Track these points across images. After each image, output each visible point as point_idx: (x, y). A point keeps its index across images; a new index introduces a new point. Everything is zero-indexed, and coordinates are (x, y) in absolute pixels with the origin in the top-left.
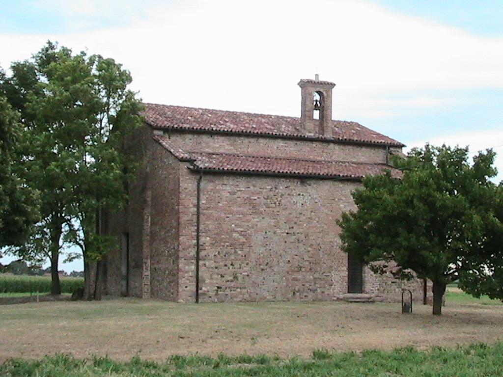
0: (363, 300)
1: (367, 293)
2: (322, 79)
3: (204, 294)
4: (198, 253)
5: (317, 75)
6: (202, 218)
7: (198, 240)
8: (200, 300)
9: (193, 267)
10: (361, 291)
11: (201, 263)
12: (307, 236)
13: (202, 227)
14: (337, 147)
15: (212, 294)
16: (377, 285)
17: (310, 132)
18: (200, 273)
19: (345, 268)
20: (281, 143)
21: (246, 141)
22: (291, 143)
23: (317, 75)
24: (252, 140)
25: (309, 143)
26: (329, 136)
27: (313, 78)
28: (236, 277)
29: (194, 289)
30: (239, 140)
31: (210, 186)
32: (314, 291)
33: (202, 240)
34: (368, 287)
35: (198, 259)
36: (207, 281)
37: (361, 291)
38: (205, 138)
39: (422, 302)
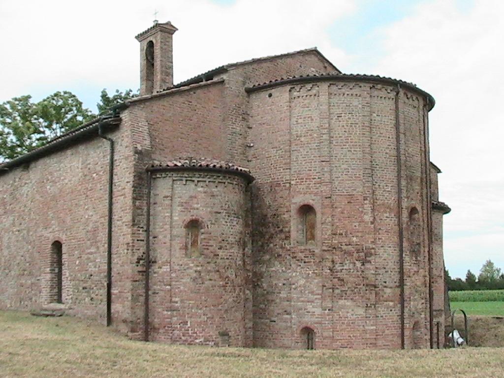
0: (47, 313)
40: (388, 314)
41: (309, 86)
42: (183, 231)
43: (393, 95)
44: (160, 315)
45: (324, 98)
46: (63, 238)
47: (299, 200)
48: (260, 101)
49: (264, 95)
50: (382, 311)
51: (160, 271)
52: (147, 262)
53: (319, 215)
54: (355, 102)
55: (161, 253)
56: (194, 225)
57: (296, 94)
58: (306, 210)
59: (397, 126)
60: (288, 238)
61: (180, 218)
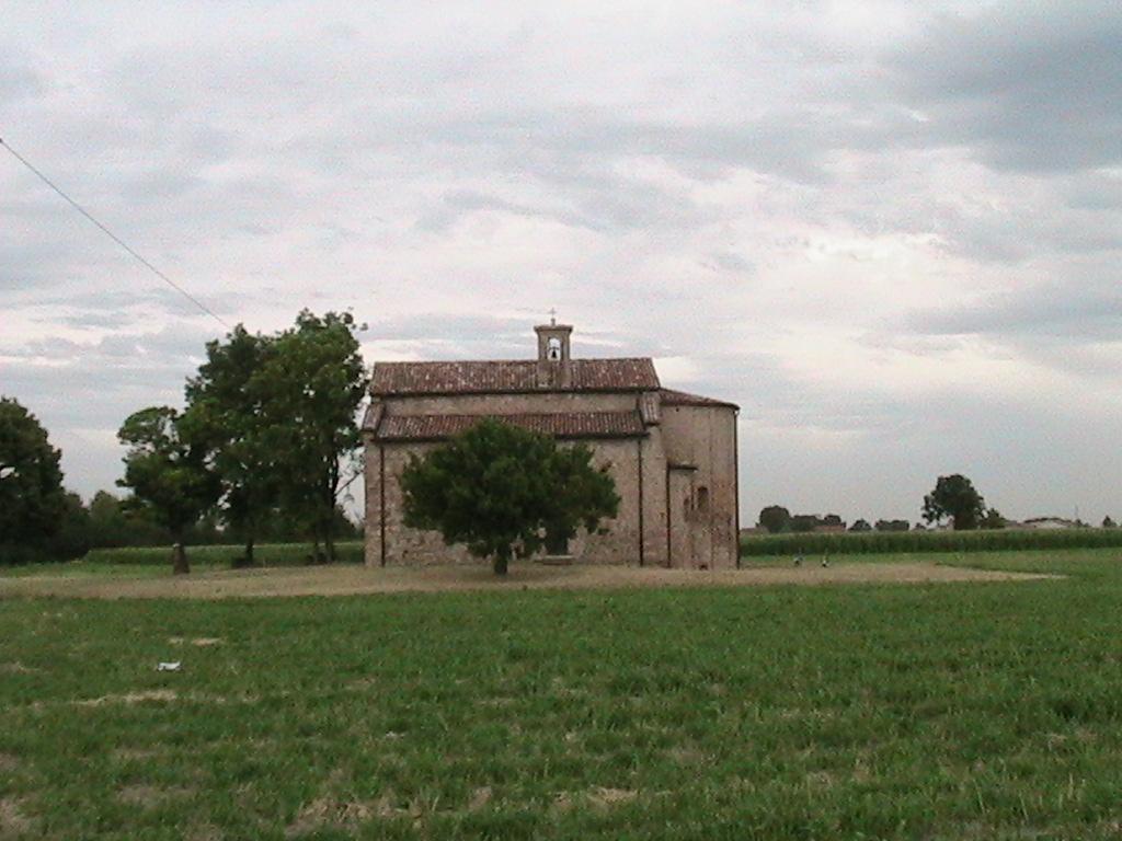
1: (571, 554)
2: (559, 322)
3: (391, 558)
4: (383, 519)
5: (553, 320)
6: (386, 485)
7: (383, 505)
8: (387, 564)
9: (379, 533)
11: (386, 529)
13: (386, 494)
14: (577, 398)
18: (386, 538)
20: (510, 399)
23: (553, 320)
24: (478, 398)
25: (543, 396)
26: (566, 385)
27: (549, 323)
28: (422, 541)
29: (380, 552)
30: (462, 400)
31: (394, 454)
33: (387, 506)
35: (383, 525)
36: (394, 545)
37: (566, 553)
56: (686, 502)
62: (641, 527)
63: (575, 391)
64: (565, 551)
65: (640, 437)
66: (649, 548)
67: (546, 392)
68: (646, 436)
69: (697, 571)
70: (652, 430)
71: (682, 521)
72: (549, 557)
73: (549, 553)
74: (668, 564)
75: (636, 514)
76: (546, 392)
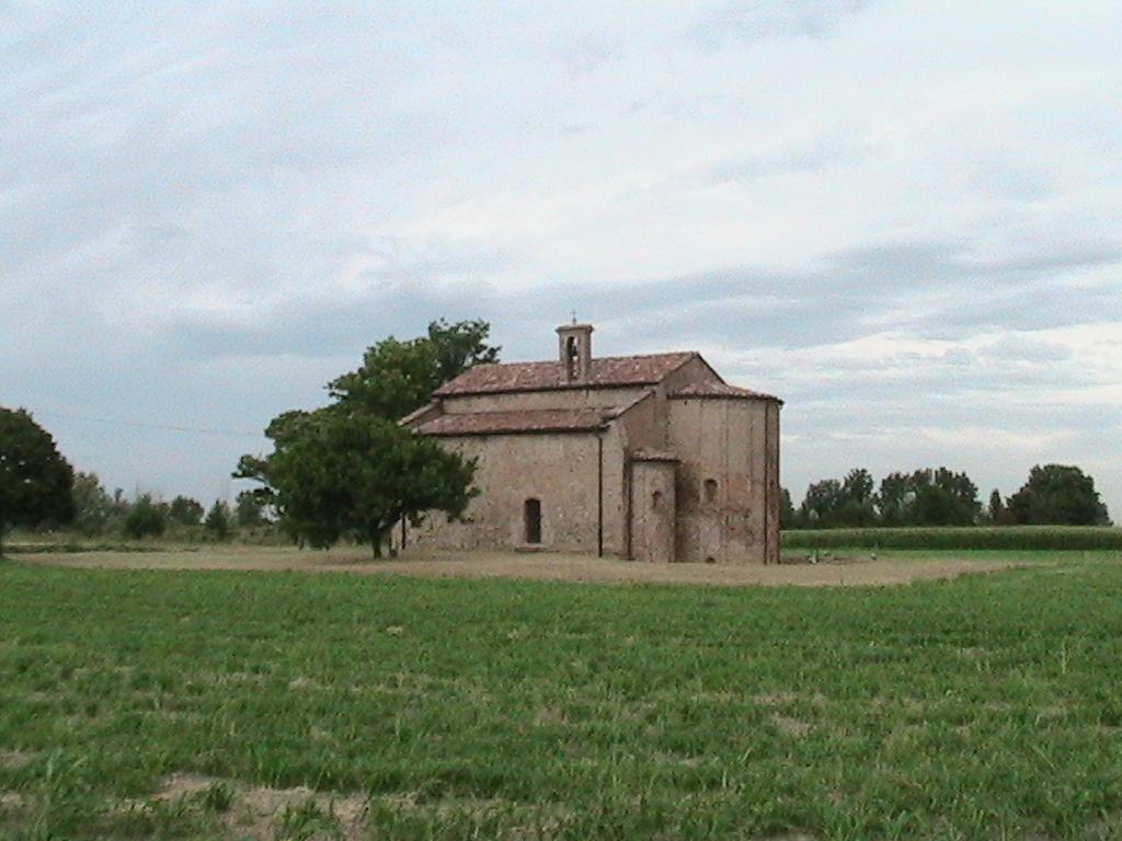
5: (574, 320)
8: (407, 546)
10: (539, 541)
12: (488, 488)
14: (591, 393)
15: (414, 542)
16: (552, 535)
17: (563, 380)
19: (521, 519)
20: (536, 396)
21: (507, 397)
22: (546, 395)
23: (574, 320)
24: (512, 396)
28: (432, 528)
30: (501, 397)
32: (495, 541)
34: (544, 537)
38: (474, 400)
39: (597, 553)
40: (758, 548)
41: (714, 401)
42: (652, 498)
43: (764, 406)
44: (637, 548)
45: (724, 409)
46: (539, 496)
47: (707, 476)
48: (677, 407)
49: (681, 402)
50: (755, 547)
51: (637, 522)
52: (630, 516)
53: (719, 486)
54: (743, 413)
55: (637, 511)
56: (656, 495)
57: (705, 405)
58: (711, 482)
59: (766, 429)
60: (698, 499)
61: (649, 490)
62: (600, 520)
63: (588, 387)
64: (539, 541)
65: (599, 431)
66: (607, 540)
67: (564, 389)
68: (605, 430)
69: (706, 566)
70: (611, 423)
71: (649, 514)
72: (527, 545)
73: (529, 541)
74: (629, 555)
75: (597, 505)
76: (564, 389)
